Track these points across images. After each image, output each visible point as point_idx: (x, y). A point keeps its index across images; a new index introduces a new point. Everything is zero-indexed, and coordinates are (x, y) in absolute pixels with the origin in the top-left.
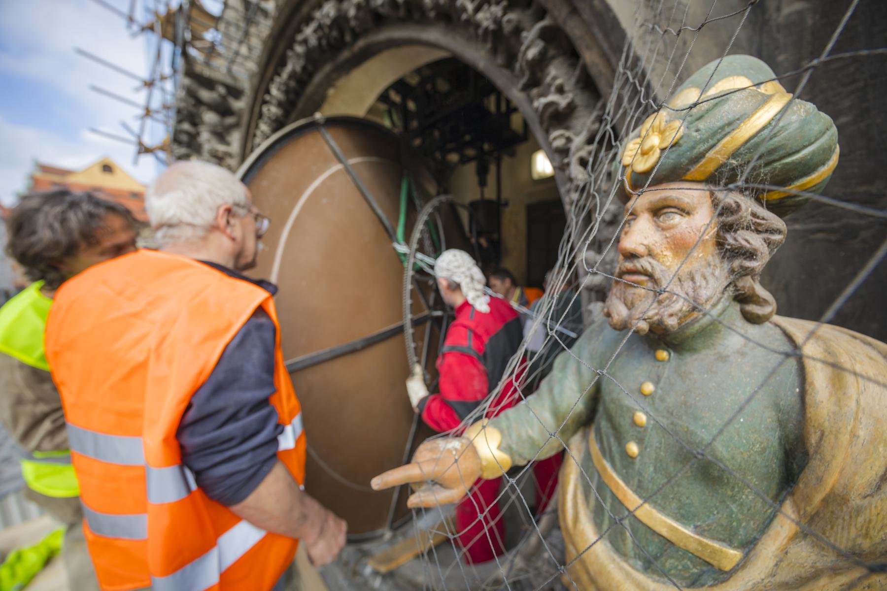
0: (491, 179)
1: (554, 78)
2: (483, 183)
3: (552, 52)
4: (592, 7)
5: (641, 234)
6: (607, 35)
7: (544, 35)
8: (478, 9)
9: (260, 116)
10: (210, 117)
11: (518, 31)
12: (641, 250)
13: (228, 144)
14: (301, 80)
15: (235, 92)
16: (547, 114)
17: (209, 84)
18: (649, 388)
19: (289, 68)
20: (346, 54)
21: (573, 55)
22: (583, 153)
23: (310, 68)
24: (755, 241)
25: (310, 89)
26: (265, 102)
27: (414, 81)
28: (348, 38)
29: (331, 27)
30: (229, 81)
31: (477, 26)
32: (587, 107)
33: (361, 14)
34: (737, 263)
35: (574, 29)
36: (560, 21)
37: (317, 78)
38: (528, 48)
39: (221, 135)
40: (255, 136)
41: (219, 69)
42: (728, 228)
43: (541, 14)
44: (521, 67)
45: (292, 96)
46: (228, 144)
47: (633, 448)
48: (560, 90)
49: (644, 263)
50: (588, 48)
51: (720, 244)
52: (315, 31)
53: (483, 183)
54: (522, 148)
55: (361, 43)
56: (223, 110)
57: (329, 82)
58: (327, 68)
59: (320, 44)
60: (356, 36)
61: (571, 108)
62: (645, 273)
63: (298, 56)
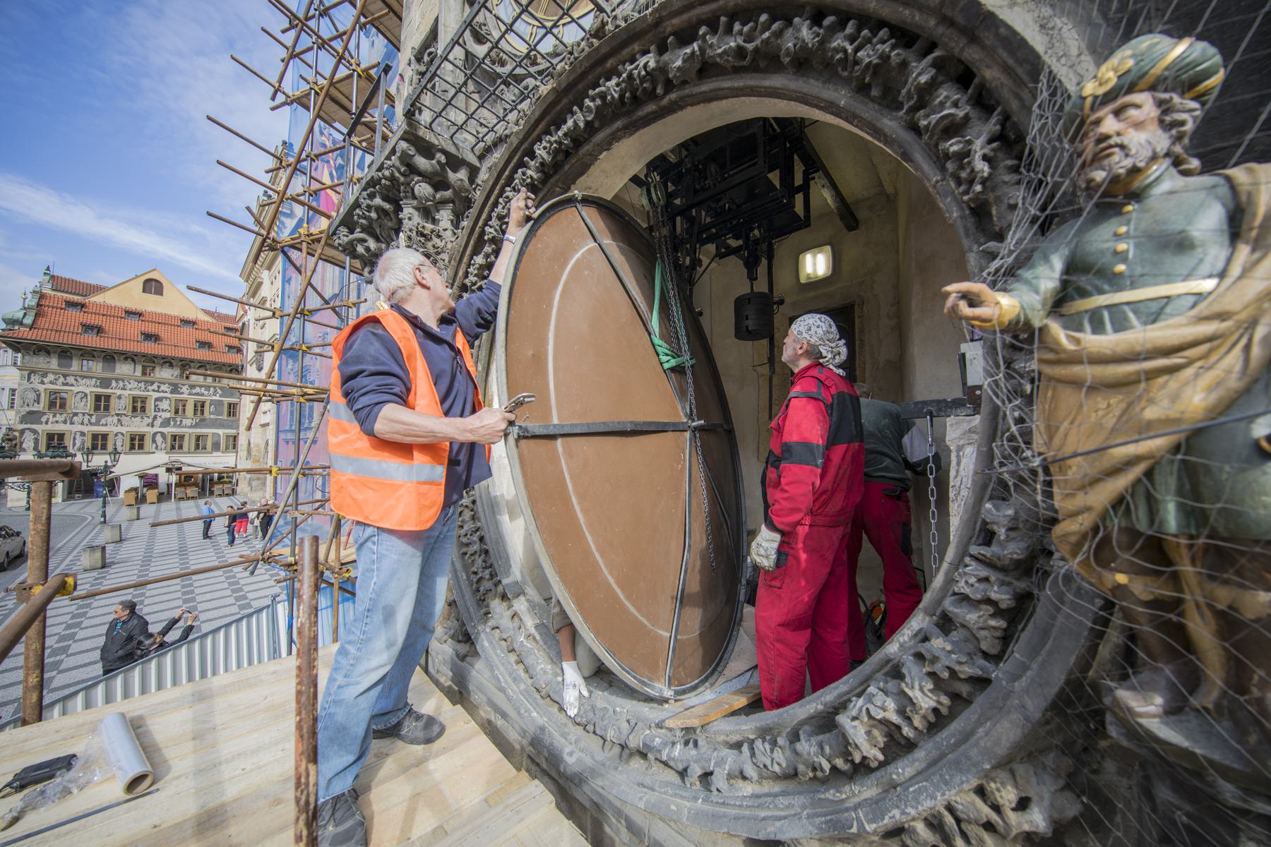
0: (762, 269)
1: (947, 97)
2: (752, 278)
3: (941, 78)
4: (997, 35)
5: (1110, 125)
6: (1012, 53)
7: (936, 64)
8: (857, 50)
9: (510, 181)
10: (423, 189)
11: (904, 65)
12: (1111, 132)
13: (434, 221)
14: (578, 139)
15: (455, 162)
16: (941, 127)
17: (427, 150)
18: (1123, 229)
19: (570, 123)
20: (651, 107)
21: (964, 77)
22: (986, 151)
23: (597, 124)
24: (1184, 116)
25: (586, 149)
26: (524, 165)
27: (673, 158)
28: (659, 91)
29: (643, 80)
30: (452, 150)
31: (856, 62)
32: (979, 119)
33: (687, 65)
34: (1174, 132)
35: (972, 54)
36: (956, 51)
37: (600, 136)
38: (920, 74)
39: (427, 213)
40: (496, 204)
41: (440, 137)
42: (1165, 112)
43: (932, 46)
44: (909, 91)
45: (560, 157)
46: (434, 221)
47: (1121, 268)
48: (955, 104)
49: (1112, 142)
50: (988, 67)
51: (1161, 122)
52: (618, 85)
53: (752, 278)
54: (794, 238)
55: (673, 96)
56: (439, 183)
57: (607, 145)
58: (619, 124)
59: (622, 96)
60: (669, 85)
61: (967, 118)
62: (1117, 145)
63: (589, 110)
